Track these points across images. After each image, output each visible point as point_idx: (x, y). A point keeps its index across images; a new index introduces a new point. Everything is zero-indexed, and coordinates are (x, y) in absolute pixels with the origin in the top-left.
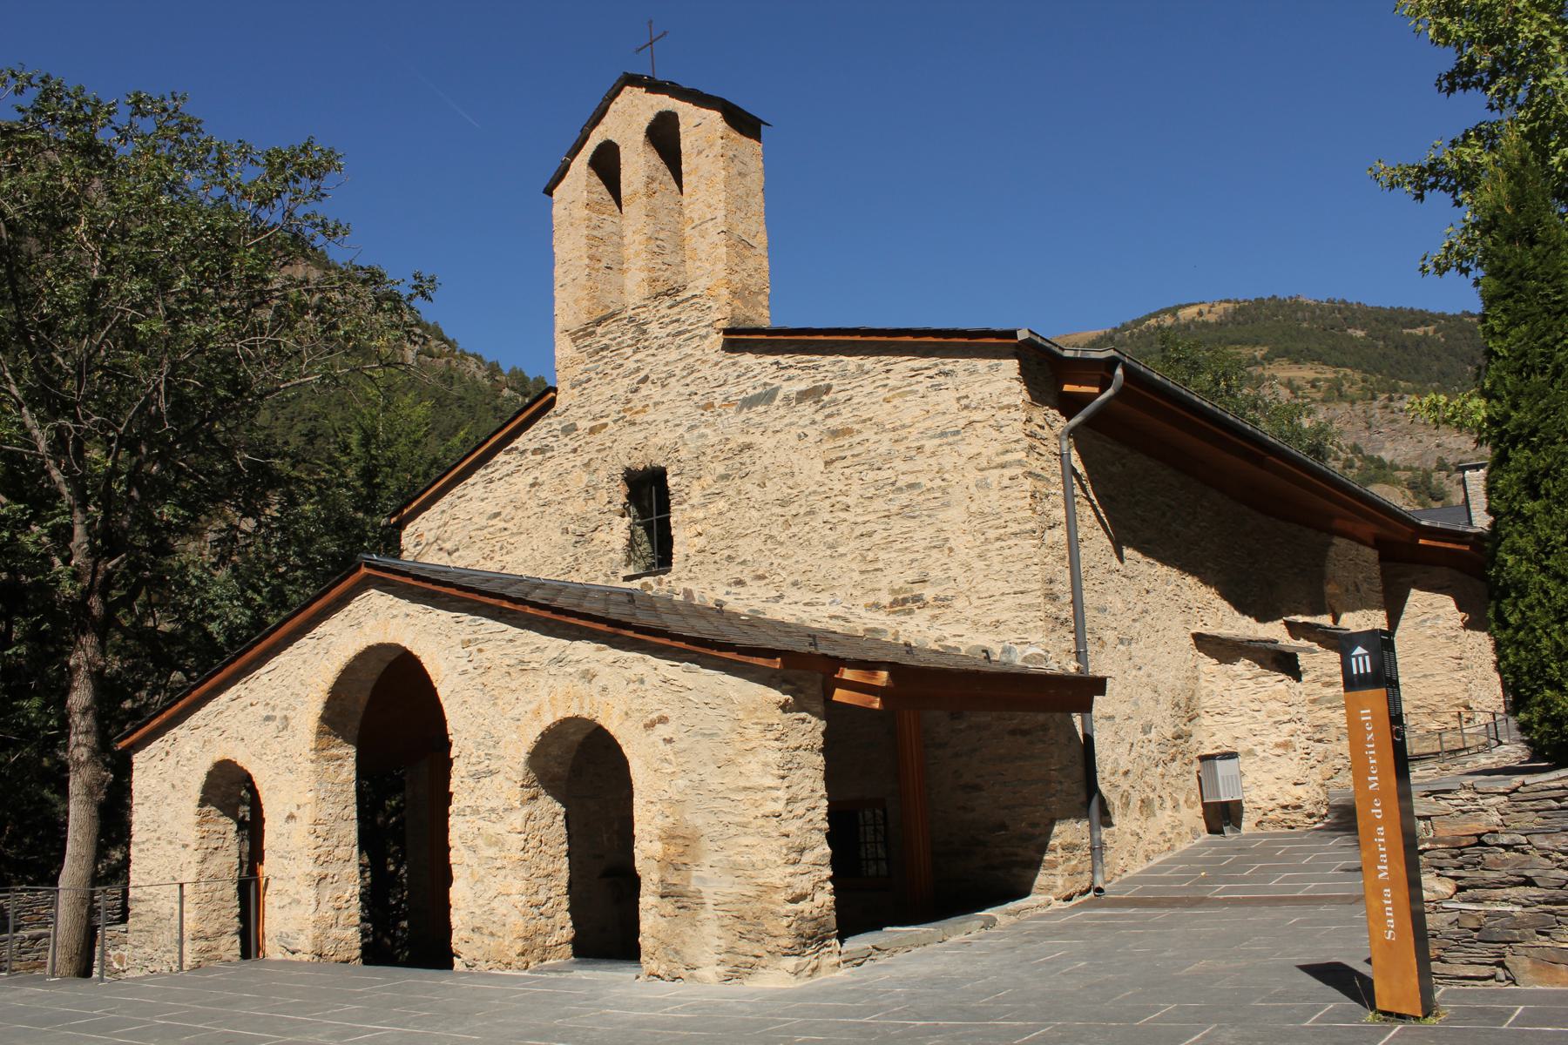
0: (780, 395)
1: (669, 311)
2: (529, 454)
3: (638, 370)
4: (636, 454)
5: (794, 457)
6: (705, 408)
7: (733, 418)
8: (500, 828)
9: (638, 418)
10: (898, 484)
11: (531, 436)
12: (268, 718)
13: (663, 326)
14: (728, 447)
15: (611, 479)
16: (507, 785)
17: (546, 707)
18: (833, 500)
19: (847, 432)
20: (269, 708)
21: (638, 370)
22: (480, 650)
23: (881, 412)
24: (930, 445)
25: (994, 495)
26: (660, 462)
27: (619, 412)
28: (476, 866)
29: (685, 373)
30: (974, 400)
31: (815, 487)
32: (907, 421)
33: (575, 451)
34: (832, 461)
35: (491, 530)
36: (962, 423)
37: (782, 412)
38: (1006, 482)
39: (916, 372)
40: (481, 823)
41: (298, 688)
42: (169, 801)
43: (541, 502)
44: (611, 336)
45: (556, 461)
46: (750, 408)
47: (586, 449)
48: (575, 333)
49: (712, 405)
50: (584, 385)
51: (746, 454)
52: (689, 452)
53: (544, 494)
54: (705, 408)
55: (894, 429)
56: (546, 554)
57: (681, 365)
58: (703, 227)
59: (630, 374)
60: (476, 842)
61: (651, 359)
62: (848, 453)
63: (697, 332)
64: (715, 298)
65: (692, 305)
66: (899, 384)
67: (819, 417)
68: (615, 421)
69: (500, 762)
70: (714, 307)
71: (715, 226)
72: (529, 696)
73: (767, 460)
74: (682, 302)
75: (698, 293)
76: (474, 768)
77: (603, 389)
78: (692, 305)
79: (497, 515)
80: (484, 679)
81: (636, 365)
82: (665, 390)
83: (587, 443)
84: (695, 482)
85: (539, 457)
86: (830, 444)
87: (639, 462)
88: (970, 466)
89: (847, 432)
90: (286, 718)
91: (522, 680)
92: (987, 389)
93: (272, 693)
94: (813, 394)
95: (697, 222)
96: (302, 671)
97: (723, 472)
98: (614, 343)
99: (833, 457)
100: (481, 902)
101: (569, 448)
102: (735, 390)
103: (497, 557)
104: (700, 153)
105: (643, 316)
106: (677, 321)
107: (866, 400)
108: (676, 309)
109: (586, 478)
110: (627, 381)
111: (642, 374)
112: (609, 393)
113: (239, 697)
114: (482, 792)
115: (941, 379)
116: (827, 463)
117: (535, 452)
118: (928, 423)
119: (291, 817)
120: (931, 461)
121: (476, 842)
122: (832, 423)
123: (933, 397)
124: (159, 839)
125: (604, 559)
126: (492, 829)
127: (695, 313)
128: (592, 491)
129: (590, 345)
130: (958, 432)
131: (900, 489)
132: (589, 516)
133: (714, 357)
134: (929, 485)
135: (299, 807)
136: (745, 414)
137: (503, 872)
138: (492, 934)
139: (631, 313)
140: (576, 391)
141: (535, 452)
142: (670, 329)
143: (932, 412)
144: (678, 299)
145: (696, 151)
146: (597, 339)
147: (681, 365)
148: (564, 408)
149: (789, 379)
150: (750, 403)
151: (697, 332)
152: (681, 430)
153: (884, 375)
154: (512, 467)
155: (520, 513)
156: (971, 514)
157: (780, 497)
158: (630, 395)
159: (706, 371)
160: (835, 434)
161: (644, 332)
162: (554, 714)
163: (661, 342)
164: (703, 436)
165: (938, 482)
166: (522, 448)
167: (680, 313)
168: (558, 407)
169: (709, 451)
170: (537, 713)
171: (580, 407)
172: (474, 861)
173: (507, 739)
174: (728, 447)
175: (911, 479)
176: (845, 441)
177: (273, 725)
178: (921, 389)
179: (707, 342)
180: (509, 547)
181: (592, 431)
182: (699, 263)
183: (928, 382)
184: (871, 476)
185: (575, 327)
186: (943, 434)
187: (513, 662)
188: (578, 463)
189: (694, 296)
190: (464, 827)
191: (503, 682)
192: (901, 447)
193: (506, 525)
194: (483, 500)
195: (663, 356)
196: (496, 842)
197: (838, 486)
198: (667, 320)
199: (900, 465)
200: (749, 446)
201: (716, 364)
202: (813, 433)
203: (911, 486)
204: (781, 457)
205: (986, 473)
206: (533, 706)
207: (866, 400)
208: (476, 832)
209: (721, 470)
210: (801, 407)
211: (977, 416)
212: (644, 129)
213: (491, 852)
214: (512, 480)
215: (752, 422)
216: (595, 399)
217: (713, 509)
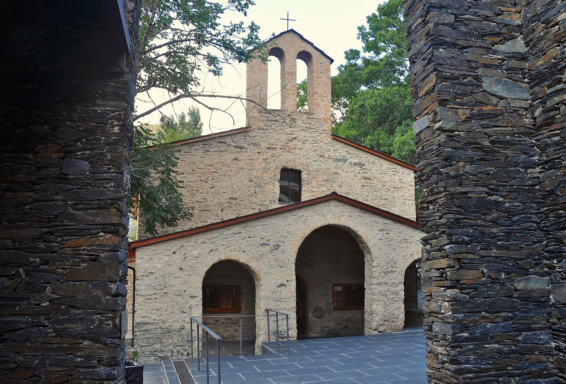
0: (348, 161)
1: (307, 119)
2: (232, 147)
3: (291, 134)
4: (290, 163)
5: (352, 181)
6: (321, 156)
7: (331, 165)
8: (396, 289)
9: (292, 151)
10: (382, 197)
12: (264, 244)
14: (329, 171)
15: (277, 168)
16: (399, 276)
17: (415, 253)
18: (363, 197)
19: (369, 179)
20: (264, 240)
21: (291, 134)
22: (388, 233)
23: (379, 176)
24: (392, 189)
25: (407, 207)
26: (299, 168)
27: (282, 146)
28: (386, 301)
29: (313, 142)
30: (404, 181)
31: (358, 192)
32: (386, 181)
33: (259, 153)
34: (364, 186)
35: (207, 170)
36: (400, 186)
37: (349, 166)
38: (410, 204)
39: (389, 169)
40: (389, 287)
41: (285, 234)
42: (176, 276)
43: (239, 167)
45: (249, 153)
46: (338, 162)
47: (265, 154)
49: (324, 156)
50: (264, 131)
51: (336, 176)
52: (313, 169)
53: (241, 164)
54: (321, 156)
55: (382, 182)
56: (239, 187)
58: (322, 97)
59: (288, 134)
60: (386, 293)
61: (298, 132)
62: (369, 185)
64: (327, 123)
66: (384, 170)
67: (361, 172)
68: (280, 149)
69: (396, 269)
72: (408, 250)
73: (343, 179)
76: (386, 270)
77: (275, 135)
79: (213, 166)
80: (389, 243)
82: (304, 145)
83: (265, 152)
84: (314, 179)
85: (240, 150)
86: (364, 181)
87: (290, 165)
88: (401, 198)
89: (369, 179)
90: (278, 245)
91: (405, 245)
92: (407, 179)
93: (266, 234)
94: (361, 165)
96: (287, 228)
97: (326, 179)
99: (365, 184)
100: (387, 312)
101: (256, 150)
102: (333, 154)
103: (210, 182)
104: (321, 73)
106: (311, 124)
107: (375, 172)
109: (264, 165)
110: (286, 136)
111: (294, 136)
112: (278, 138)
113: (240, 233)
114: (388, 278)
115: (395, 173)
116: (362, 186)
117: (235, 147)
118: (391, 183)
119: (282, 285)
120: (392, 194)
121: (386, 293)
122: (365, 175)
123: (393, 177)
124: (166, 293)
125: (270, 195)
126: (393, 289)
127: (318, 124)
128: (266, 170)
130: (399, 188)
131: (383, 199)
132: (264, 178)
133: (326, 142)
134: (391, 200)
135: (288, 281)
136: (336, 163)
137: (398, 302)
138: (393, 321)
140: (261, 131)
141: (236, 147)
142: (307, 125)
143: (393, 181)
145: (320, 71)
149: (351, 157)
150: (339, 160)
152: (310, 160)
153: (380, 166)
154: (222, 149)
155: (225, 168)
156: (401, 210)
157: (346, 191)
159: (322, 144)
160: (365, 178)
161: (295, 122)
162: (418, 256)
163: (303, 128)
164: (321, 165)
165: (392, 200)
166: (228, 143)
169: (321, 170)
170: (412, 255)
171: (262, 137)
172: (385, 299)
173: (400, 262)
174: (329, 171)
175: (386, 197)
176: (369, 181)
177: (268, 248)
178: (390, 174)
179: (322, 135)
180: (217, 180)
181: (268, 148)
183: (392, 173)
184: (375, 193)
186: (395, 188)
187: (401, 239)
188: (261, 157)
189: (317, 119)
190: (381, 289)
191: (398, 245)
192: (384, 188)
193: (216, 171)
194: (202, 157)
195: (302, 132)
196: (396, 293)
197: (365, 194)
198: (306, 122)
199: (384, 193)
200: (337, 173)
201: (326, 144)
202: (359, 176)
203: (386, 199)
204: (348, 180)
205: (405, 201)
206: (411, 253)
207: (375, 172)
208: (386, 290)
209: (325, 178)
210: (355, 167)
211: (404, 185)
212: (298, 53)
213: (393, 296)
214: (221, 154)
215: (339, 166)
217: (320, 189)
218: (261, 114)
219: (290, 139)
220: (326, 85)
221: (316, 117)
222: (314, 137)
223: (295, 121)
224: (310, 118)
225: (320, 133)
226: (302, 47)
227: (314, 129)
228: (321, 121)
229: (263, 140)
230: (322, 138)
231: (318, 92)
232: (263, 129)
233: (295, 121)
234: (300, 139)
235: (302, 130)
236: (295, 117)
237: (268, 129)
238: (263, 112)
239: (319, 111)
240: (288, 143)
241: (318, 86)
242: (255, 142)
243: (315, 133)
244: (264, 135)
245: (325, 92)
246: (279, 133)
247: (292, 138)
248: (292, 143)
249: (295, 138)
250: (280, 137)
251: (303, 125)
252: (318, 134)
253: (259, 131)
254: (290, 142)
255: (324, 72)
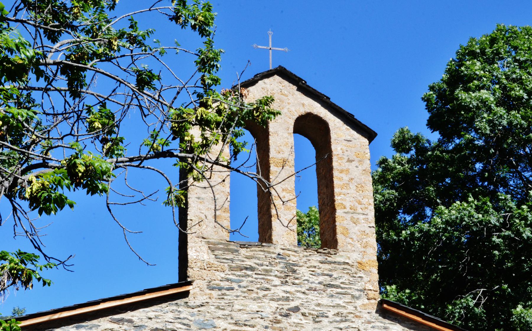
1: (321, 265)
3: (287, 299)
11: (152, 315)
13: (313, 274)
21: (287, 299)
44: (258, 262)
48: (214, 244)
50: (224, 291)
57: (336, 311)
58: (356, 216)
59: (279, 300)
61: (302, 296)
63: (348, 291)
65: (344, 269)
70: (366, 279)
71: (367, 220)
74: (334, 263)
75: (350, 263)
77: (247, 302)
78: (344, 269)
81: (285, 295)
95: (348, 209)
98: (260, 268)
105: (293, 258)
106: (331, 276)
108: (327, 266)
110: (274, 304)
111: (293, 304)
127: (347, 277)
129: (232, 260)
133: (367, 316)
139: (278, 251)
140: (215, 293)
142: (321, 279)
144: (329, 259)
146: (240, 258)
147: (336, 311)
148: (198, 303)
151: (348, 291)
158: (279, 318)
161: (294, 271)
163: (313, 285)
166: (137, 322)
167: (330, 270)
168: (190, 300)
171: (218, 308)
179: (359, 303)
182: (350, 241)
185: (214, 238)
189: (345, 263)
195: (312, 296)
198: (319, 271)
201: (369, 322)
216: (237, 307)
218: (216, 253)
219: (284, 311)
220: (360, 187)
221: (342, 260)
222: (338, 306)
223: (295, 268)
224: (330, 263)
225: (353, 297)
226: (303, 105)
227: (337, 287)
228: (354, 270)
229: (220, 313)
230: (358, 308)
231: (344, 203)
232: (220, 289)
233: (295, 268)
234: (306, 311)
235: (310, 289)
236: (293, 258)
237: (232, 289)
238: (219, 249)
239: (349, 247)
240: (278, 322)
241: (344, 191)
242: (202, 318)
243: (341, 296)
244: (223, 302)
245: (360, 203)
246: (259, 298)
247: (289, 310)
248: (289, 320)
249: (296, 309)
250: (260, 307)
251: (313, 279)
252: (348, 298)
253: (213, 292)
254: (284, 319)
255: (356, 159)
